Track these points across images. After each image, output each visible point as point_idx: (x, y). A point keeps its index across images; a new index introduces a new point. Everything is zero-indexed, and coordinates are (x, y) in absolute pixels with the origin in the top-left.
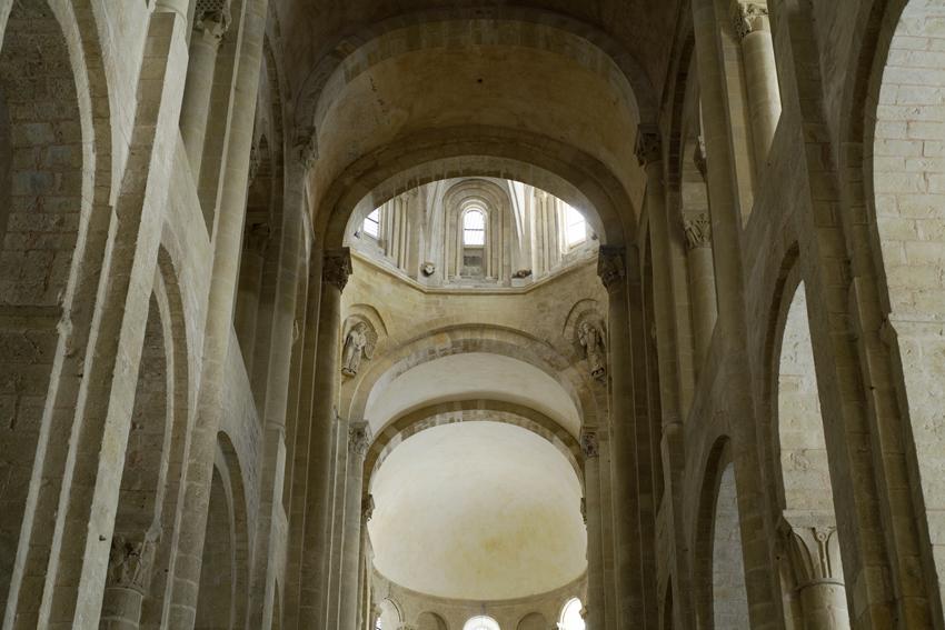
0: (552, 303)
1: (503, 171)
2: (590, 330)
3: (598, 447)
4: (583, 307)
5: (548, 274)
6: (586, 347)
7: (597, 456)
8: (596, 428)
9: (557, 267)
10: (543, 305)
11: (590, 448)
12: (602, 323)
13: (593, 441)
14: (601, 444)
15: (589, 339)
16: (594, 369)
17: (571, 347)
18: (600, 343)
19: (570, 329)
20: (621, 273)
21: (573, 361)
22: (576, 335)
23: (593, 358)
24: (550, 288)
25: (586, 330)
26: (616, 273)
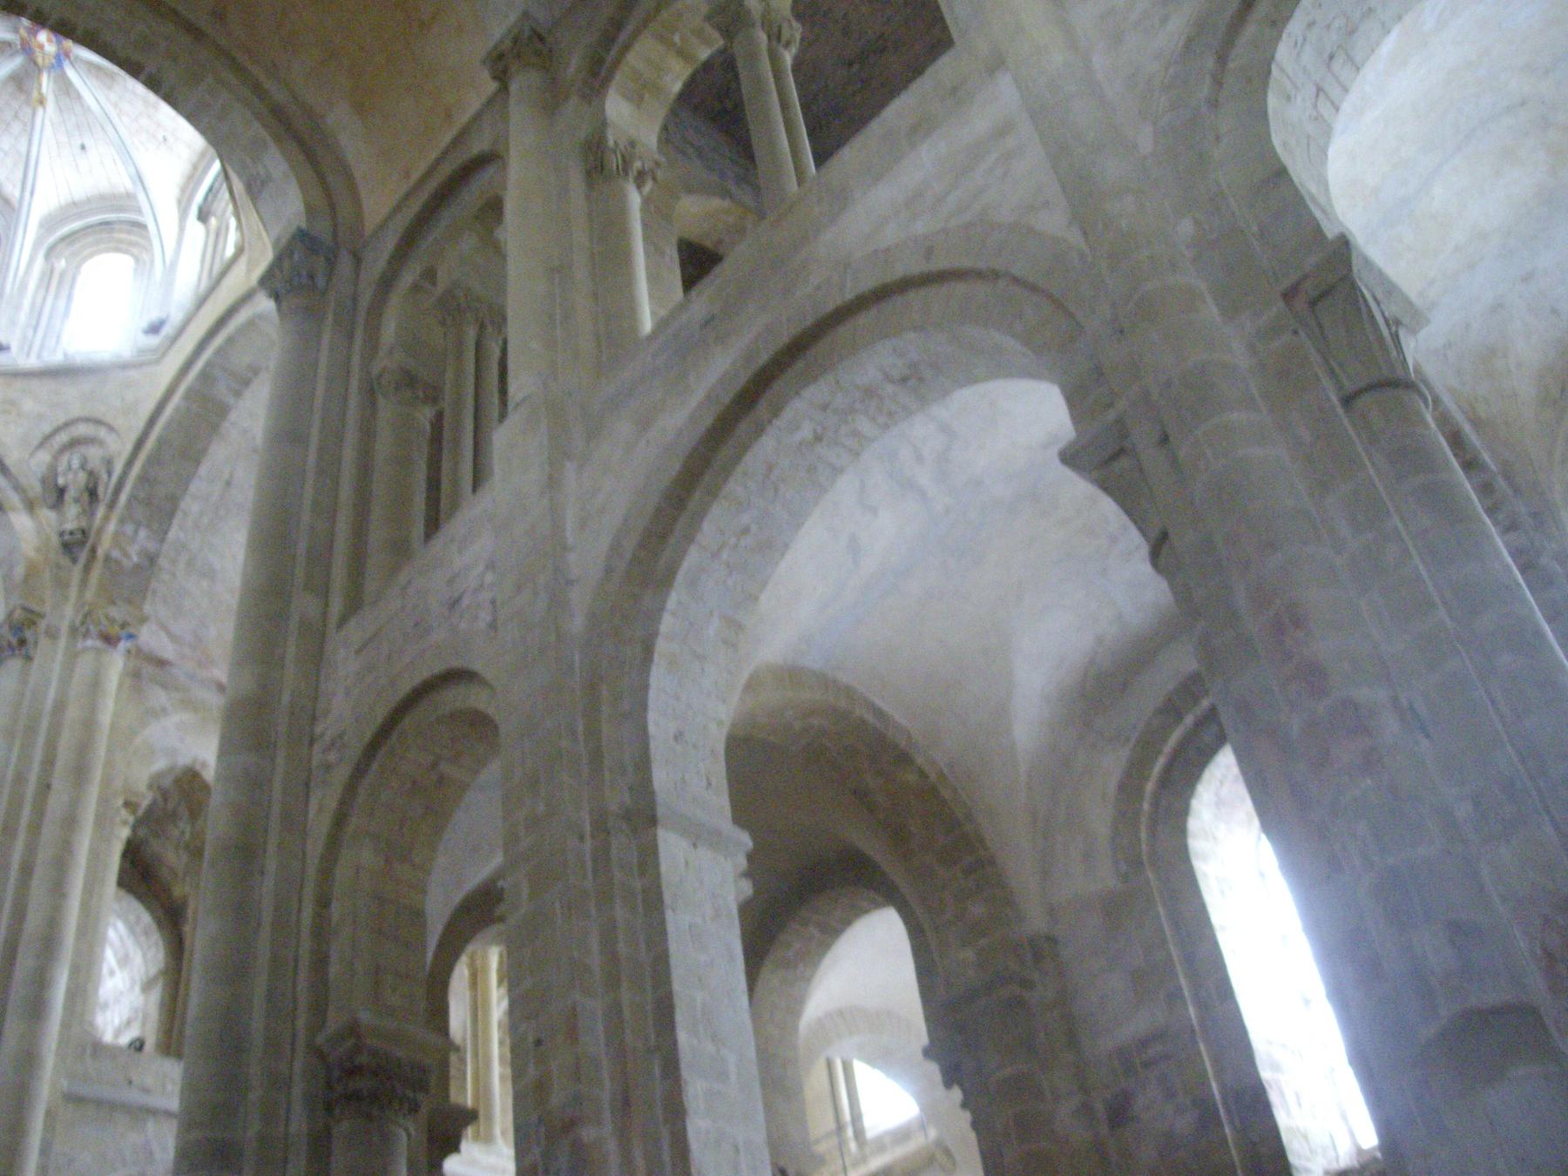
0: (28, 405)
1: (150, 68)
2: (83, 467)
3: (36, 643)
4: (82, 430)
5: (32, 362)
6: (61, 492)
7: (29, 658)
8: (42, 616)
9: (55, 358)
10: (12, 403)
11: (22, 642)
12: (109, 463)
13: (28, 634)
14: (44, 642)
15: (75, 481)
16: (69, 526)
17: (35, 488)
18: (92, 493)
19: (44, 457)
20: (321, 282)
21: (30, 506)
22: (53, 470)
23: (72, 510)
24: (35, 384)
25: (76, 463)
26: (311, 277)
